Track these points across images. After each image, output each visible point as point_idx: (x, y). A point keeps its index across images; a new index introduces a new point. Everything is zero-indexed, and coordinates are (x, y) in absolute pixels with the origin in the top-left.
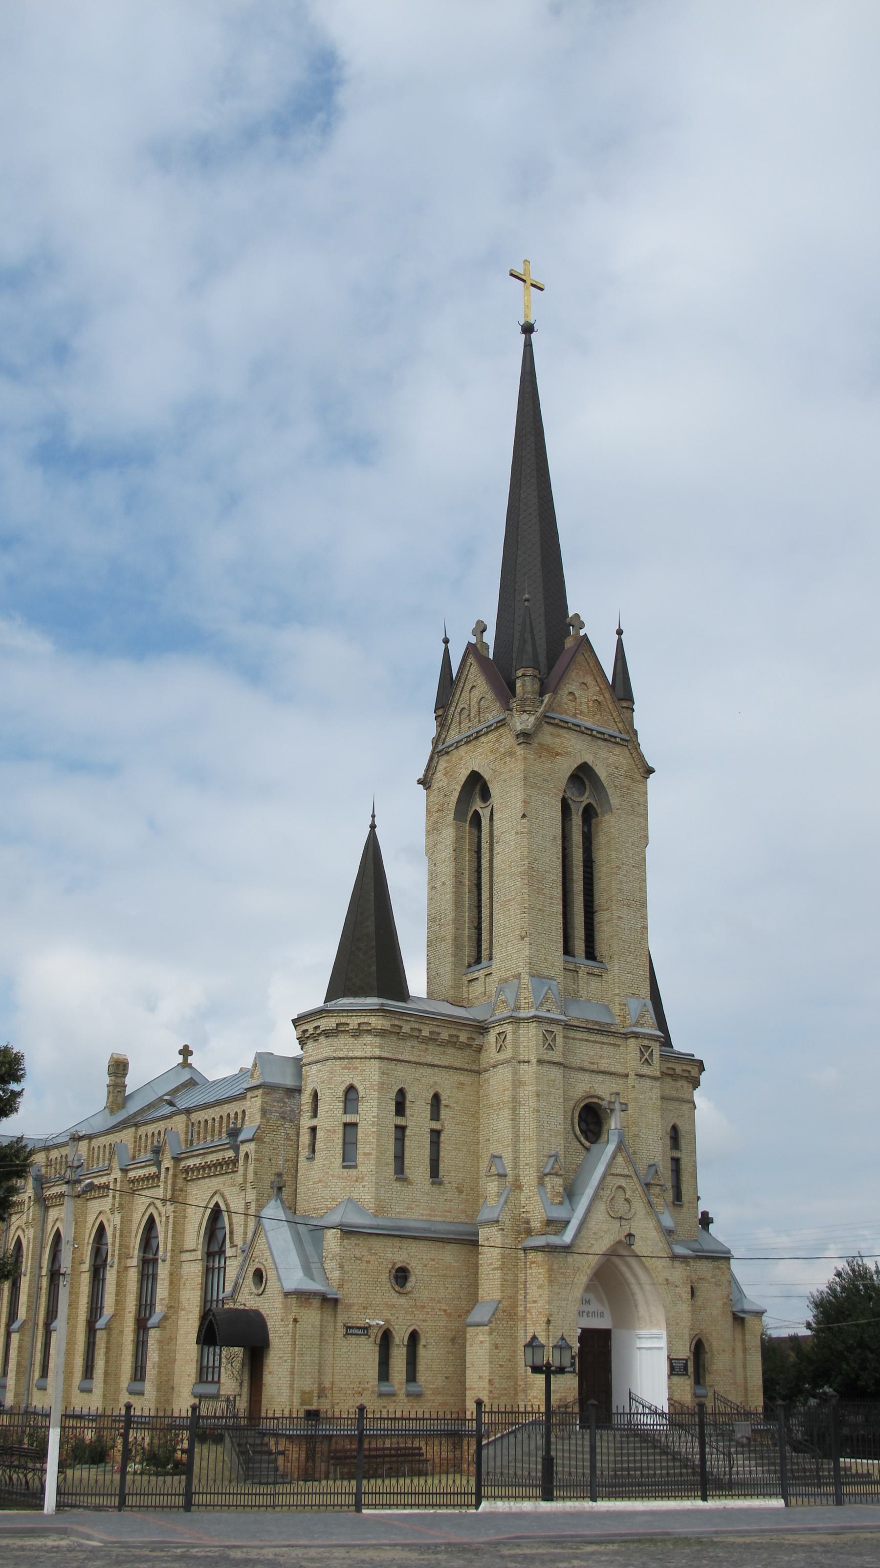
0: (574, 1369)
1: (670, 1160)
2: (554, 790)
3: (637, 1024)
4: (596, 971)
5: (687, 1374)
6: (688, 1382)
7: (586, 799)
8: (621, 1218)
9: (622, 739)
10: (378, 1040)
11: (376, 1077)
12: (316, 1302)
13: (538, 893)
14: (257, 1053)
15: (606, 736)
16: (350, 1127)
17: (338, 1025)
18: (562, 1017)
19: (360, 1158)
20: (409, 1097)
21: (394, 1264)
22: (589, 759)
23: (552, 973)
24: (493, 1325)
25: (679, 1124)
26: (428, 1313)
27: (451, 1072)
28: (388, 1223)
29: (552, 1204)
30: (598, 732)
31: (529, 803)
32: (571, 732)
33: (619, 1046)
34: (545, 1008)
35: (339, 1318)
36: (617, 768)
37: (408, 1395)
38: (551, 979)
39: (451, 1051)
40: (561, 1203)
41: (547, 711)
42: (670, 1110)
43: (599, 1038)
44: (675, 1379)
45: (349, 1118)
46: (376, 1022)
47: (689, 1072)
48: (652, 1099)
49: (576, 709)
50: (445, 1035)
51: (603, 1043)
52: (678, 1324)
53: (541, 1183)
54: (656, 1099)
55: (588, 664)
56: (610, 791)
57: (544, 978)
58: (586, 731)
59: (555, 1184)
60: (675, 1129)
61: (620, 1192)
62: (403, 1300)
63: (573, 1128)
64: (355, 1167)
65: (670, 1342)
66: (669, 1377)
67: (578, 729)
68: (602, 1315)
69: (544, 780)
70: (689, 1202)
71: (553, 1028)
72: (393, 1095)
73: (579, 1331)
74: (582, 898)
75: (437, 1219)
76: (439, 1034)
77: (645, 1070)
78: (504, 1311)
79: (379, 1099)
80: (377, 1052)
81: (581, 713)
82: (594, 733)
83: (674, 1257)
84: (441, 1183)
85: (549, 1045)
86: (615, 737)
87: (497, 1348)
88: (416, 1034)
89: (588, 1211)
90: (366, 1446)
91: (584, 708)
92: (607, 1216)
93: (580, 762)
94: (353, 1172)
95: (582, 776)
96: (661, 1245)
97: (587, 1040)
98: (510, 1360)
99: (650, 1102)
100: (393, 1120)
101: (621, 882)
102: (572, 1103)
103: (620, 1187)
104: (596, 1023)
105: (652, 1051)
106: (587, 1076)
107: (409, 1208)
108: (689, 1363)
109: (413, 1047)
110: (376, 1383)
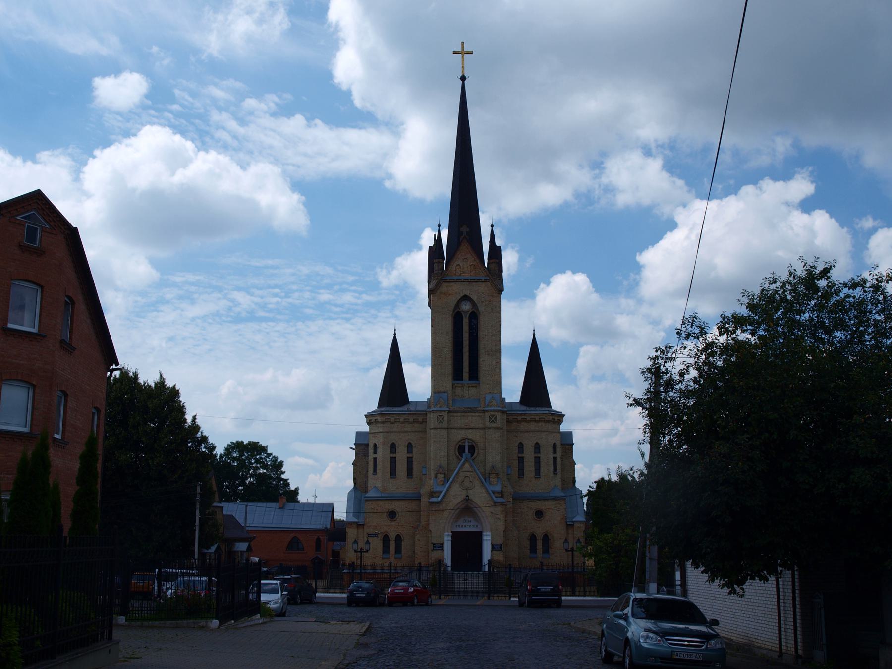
1: (534, 459)
2: (448, 311)
3: (488, 406)
4: (473, 385)
5: (501, 550)
6: (502, 553)
9: (485, 280)
10: (382, 425)
11: (381, 440)
12: (355, 526)
13: (439, 358)
14: (357, 432)
15: (476, 281)
16: (375, 459)
17: (370, 420)
18: (448, 409)
19: (378, 471)
20: (397, 445)
21: (389, 510)
22: (467, 293)
23: (446, 390)
24: (417, 532)
25: (539, 442)
27: (417, 433)
28: (386, 495)
29: (438, 485)
30: (471, 280)
31: (434, 320)
32: (457, 283)
33: (481, 416)
35: (365, 531)
36: (483, 293)
37: (395, 558)
38: (446, 393)
39: (416, 425)
40: (443, 484)
41: (443, 277)
42: (534, 436)
44: (494, 552)
45: (375, 456)
46: (379, 419)
47: (544, 418)
48: (495, 437)
49: (461, 271)
50: (411, 419)
51: (472, 416)
52: (497, 530)
53: (436, 477)
54: (498, 437)
55: (468, 249)
56: (478, 305)
58: (465, 281)
59: (441, 476)
60: (537, 443)
62: (393, 523)
63: (455, 453)
64: (376, 474)
65: (492, 538)
66: (491, 551)
67: (460, 281)
68: (477, 526)
69: (442, 308)
70: (545, 476)
71: (442, 414)
72: (389, 446)
73: (451, 534)
74: (468, 354)
75: (410, 492)
76: (409, 419)
77: (492, 425)
79: (383, 448)
80: (381, 430)
81: (464, 272)
82: (469, 281)
83: (495, 503)
84: (412, 478)
86: (481, 280)
88: (398, 420)
89: (450, 487)
90: (392, 577)
91: (465, 270)
93: (462, 295)
94: (376, 476)
97: (463, 416)
98: (425, 545)
100: (389, 455)
103: (466, 477)
104: (469, 408)
106: (463, 431)
107: (396, 488)
109: (398, 426)
110: (381, 554)
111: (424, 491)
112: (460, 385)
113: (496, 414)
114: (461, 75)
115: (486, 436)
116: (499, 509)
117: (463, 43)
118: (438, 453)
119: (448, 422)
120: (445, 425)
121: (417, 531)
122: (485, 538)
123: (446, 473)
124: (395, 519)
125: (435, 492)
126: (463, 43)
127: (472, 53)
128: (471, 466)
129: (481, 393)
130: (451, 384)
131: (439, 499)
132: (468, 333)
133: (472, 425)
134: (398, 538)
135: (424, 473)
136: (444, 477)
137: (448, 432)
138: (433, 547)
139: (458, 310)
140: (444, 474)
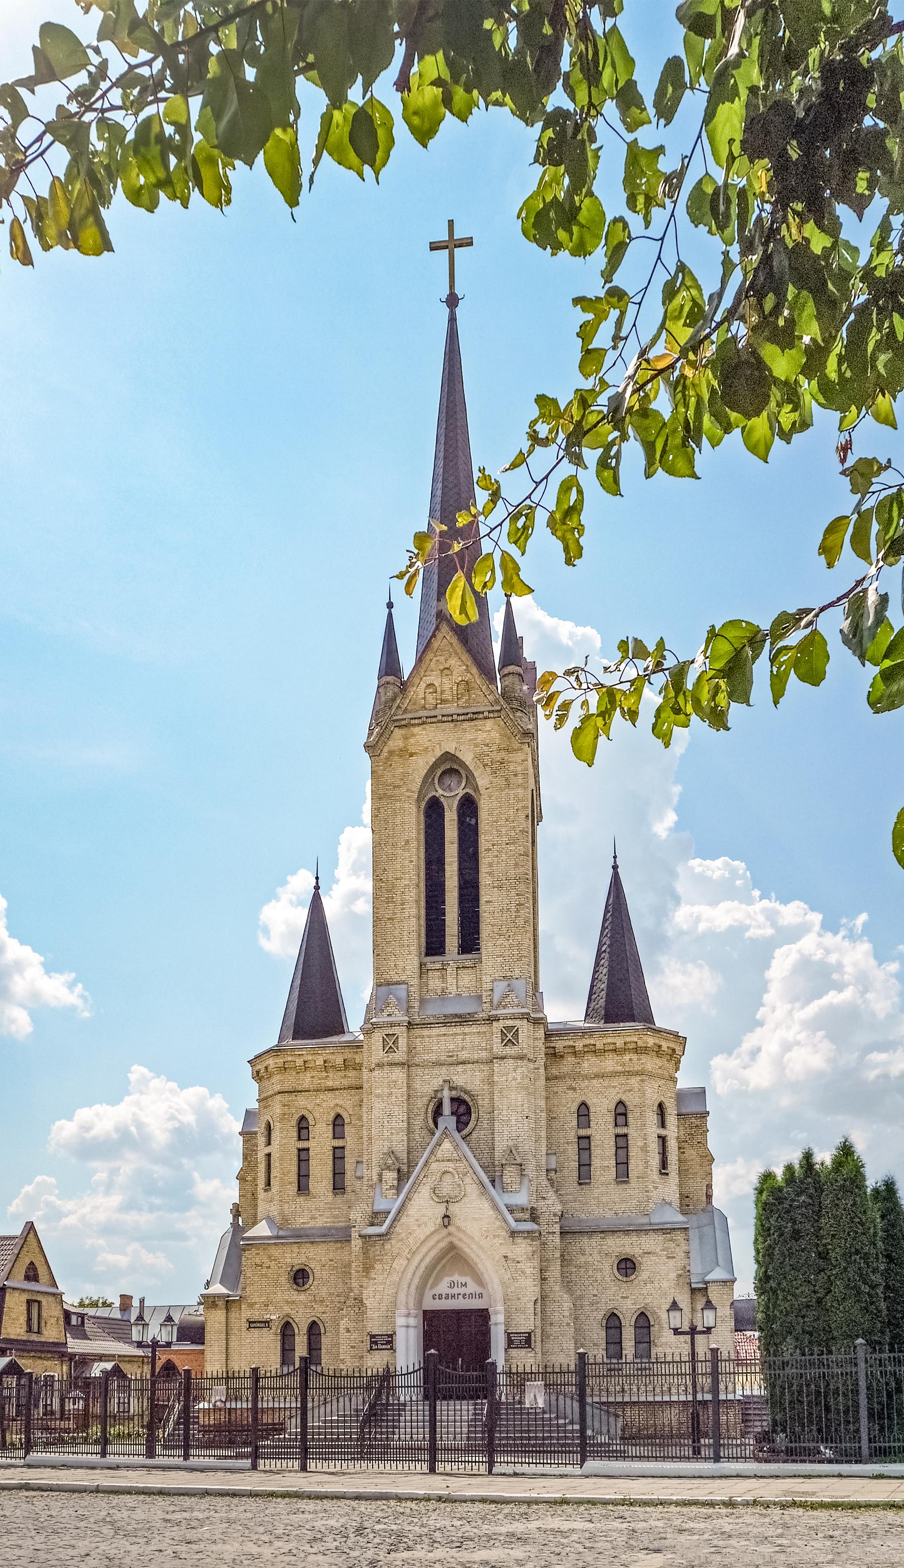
0: (391, 1348)
5: (530, 1347)
7: (461, 792)
8: (447, 1202)
13: (388, 903)
18: (407, 1018)
23: (403, 978)
24: (344, 1312)
26: (327, 1306)
33: (485, 1032)
34: (385, 1014)
43: (458, 1030)
44: (514, 1352)
48: (516, 1079)
52: (519, 1299)
57: (393, 984)
59: (390, 1177)
61: (447, 1178)
62: (302, 1297)
71: (396, 1030)
78: (355, 1299)
85: (391, 1047)
87: (348, 1331)
92: (431, 1202)
95: (456, 767)
96: (498, 1223)
99: (513, 1083)
101: (490, 865)
102: (425, 1100)
105: (517, 1030)
108: (533, 1336)
111: (358, 1215)
112: (438, 966)
113: (517, 1023)
114: (445, 292)
115: (496, 1079)
116: (522, 1248)
117: (451, 223)
118: (386, 1124)
119: (409, 1052)
120: (400, 1055)
121: (342, 1310)
122: (493, 1319)
123: (405, 1168)
124: (307, 1286)
125: (376, 1214)
126: (451, 223)
127: (471, 244)
128: (457, 1147)
129: (484, 978)
130: (416, 963)
131: (383, 1229)
132: (456, 845)
133: (464, 1055)
134: (314, 1330)
135: (358, 1174)
136: (399, 1179)
137: (408, 1076)
138: (372, 1342)
139: (434, 793)
140: (399, 1171)
